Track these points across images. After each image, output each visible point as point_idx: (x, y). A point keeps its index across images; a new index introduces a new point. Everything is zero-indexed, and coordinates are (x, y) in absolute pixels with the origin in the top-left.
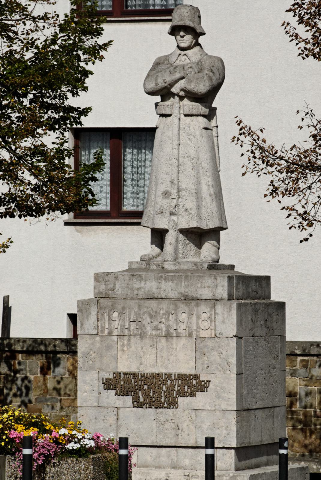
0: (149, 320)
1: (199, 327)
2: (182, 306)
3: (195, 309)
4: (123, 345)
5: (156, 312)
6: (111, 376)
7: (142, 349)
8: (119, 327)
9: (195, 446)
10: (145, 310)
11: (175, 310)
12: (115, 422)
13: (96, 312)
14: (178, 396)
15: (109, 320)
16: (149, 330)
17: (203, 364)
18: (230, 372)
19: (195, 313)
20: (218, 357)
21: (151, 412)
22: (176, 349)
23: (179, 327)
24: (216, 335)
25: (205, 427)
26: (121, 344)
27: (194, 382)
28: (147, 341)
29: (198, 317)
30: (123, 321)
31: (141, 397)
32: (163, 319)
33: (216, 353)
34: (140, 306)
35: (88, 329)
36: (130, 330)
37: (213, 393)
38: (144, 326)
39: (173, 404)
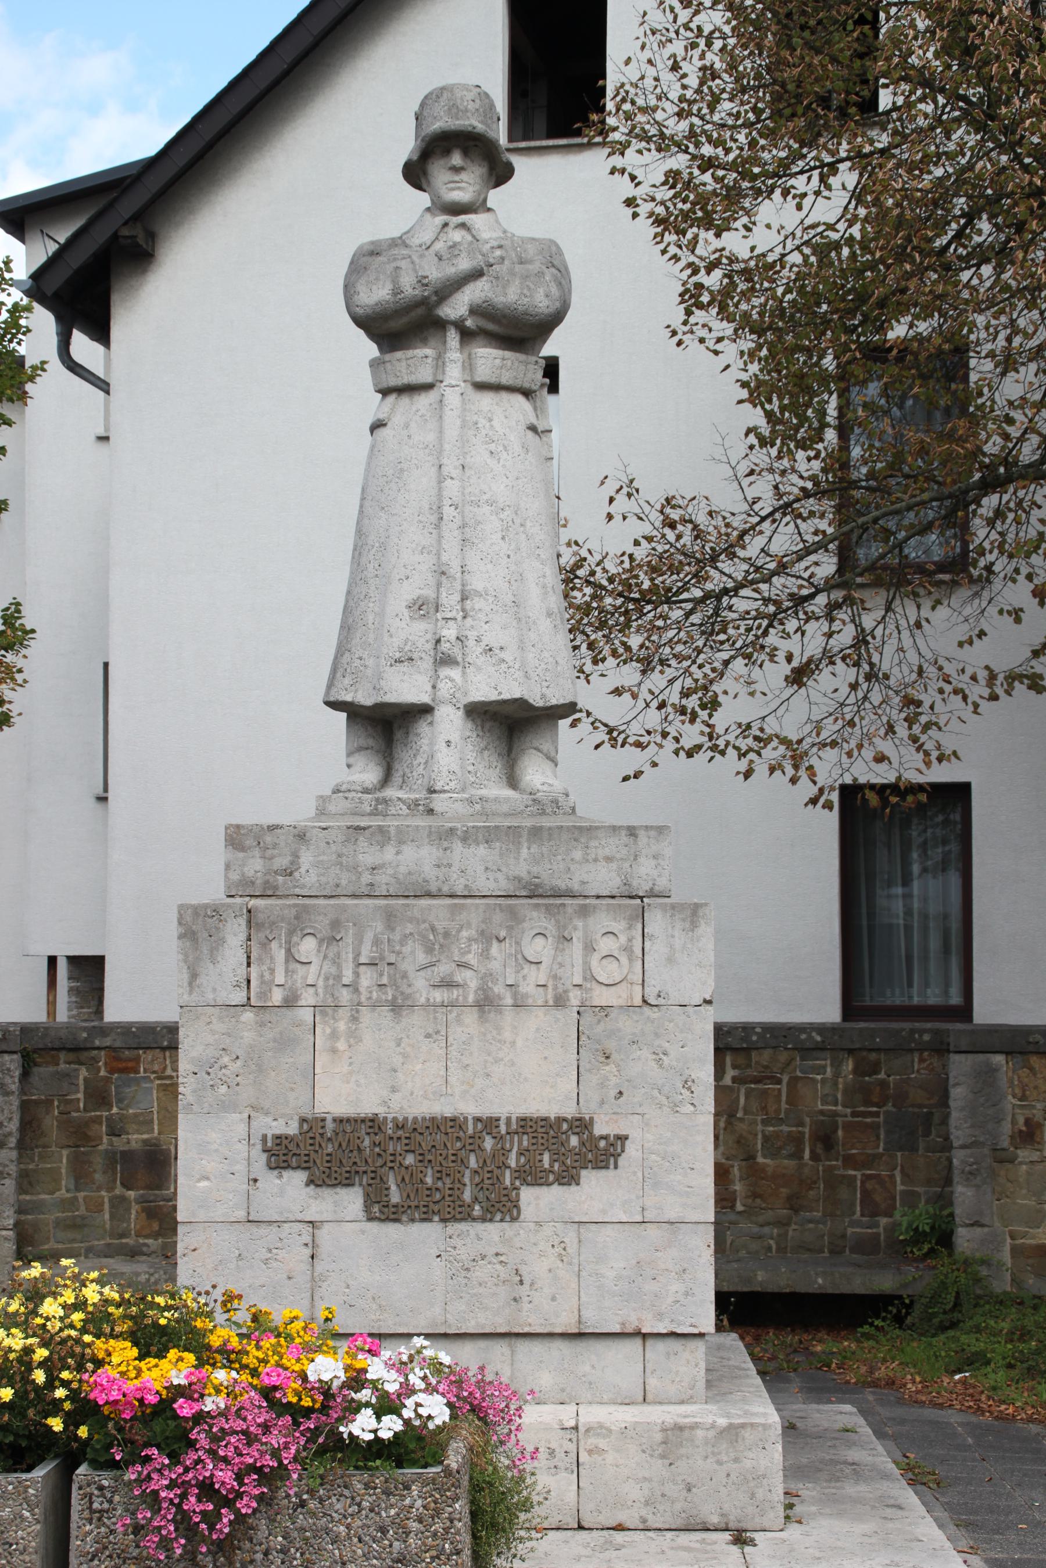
0: (422, 958)
1: (589, 976)
2: (535, 914)
3: (580, 924)
4: (334, 1035)
5: (447, 934)
6: (293, 1129)
7: (399, 1045)
8: (321, 983)
9: (576, 1331)
10: (410, 928)
11: (510, 928)
12: (305, 1267)
13: (243, 936)
14: (517, 1183)
15: (287, 961)
16: (421, 987)
17: (602, 1085)
18: (692, 1108)
19: (577, 936)
20: (653, 1064)
21: (425, 1236)
22: (513, 1043)
23: (524, 977)
24: (644, 1001)
25: (611, 1274)
26: (328, 1031)
27: (574, 1141)
28: (416, 1021)
29: (589, 948)
30: (337, 962)
31: (393, 1187)
32: (471, 956)
33: (646, 1053)
34: (390, 918)
35: (214, 990)
36: (356, 990)
37: (635, 1173)
38: (405, 976)
39: (502, 1207)
